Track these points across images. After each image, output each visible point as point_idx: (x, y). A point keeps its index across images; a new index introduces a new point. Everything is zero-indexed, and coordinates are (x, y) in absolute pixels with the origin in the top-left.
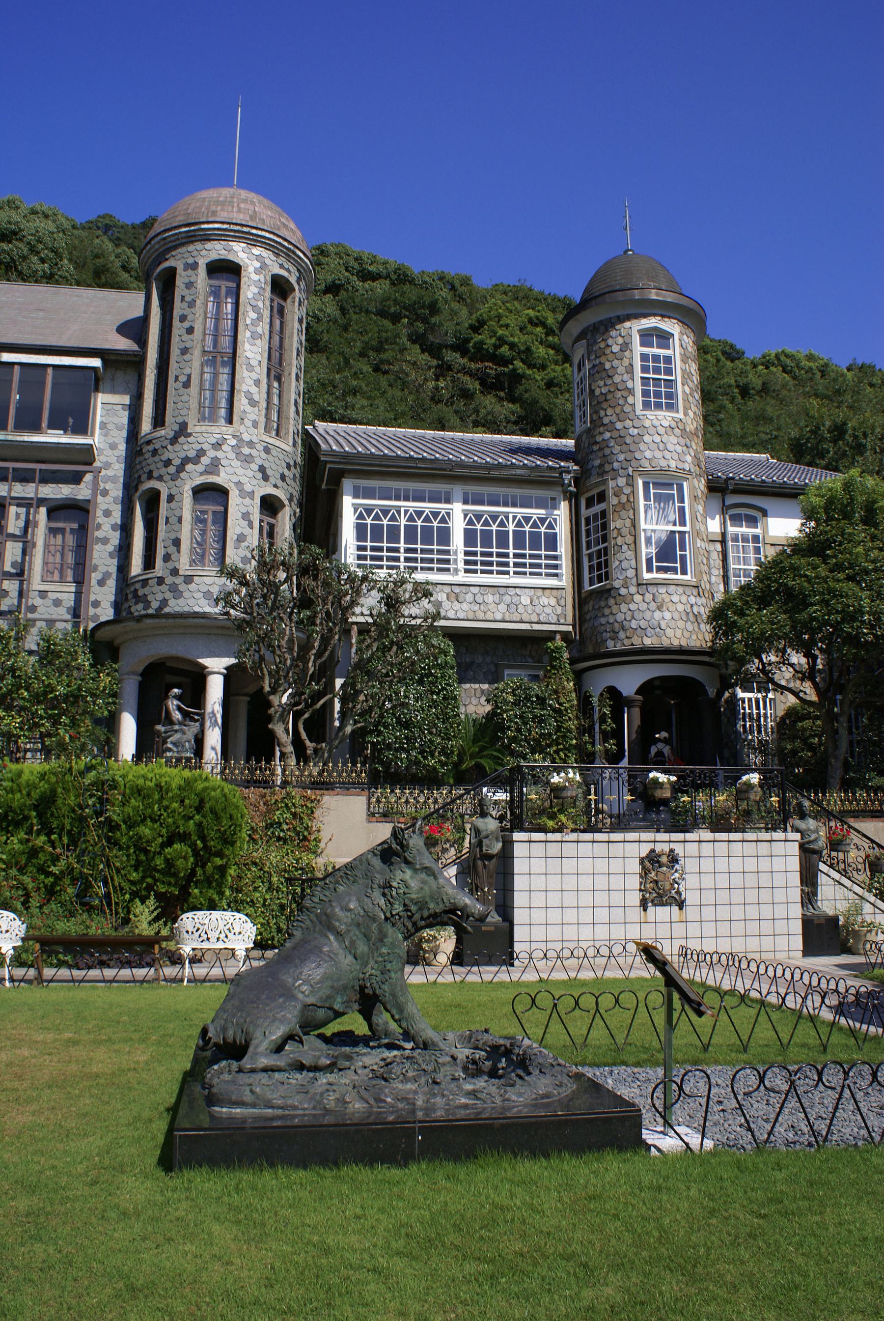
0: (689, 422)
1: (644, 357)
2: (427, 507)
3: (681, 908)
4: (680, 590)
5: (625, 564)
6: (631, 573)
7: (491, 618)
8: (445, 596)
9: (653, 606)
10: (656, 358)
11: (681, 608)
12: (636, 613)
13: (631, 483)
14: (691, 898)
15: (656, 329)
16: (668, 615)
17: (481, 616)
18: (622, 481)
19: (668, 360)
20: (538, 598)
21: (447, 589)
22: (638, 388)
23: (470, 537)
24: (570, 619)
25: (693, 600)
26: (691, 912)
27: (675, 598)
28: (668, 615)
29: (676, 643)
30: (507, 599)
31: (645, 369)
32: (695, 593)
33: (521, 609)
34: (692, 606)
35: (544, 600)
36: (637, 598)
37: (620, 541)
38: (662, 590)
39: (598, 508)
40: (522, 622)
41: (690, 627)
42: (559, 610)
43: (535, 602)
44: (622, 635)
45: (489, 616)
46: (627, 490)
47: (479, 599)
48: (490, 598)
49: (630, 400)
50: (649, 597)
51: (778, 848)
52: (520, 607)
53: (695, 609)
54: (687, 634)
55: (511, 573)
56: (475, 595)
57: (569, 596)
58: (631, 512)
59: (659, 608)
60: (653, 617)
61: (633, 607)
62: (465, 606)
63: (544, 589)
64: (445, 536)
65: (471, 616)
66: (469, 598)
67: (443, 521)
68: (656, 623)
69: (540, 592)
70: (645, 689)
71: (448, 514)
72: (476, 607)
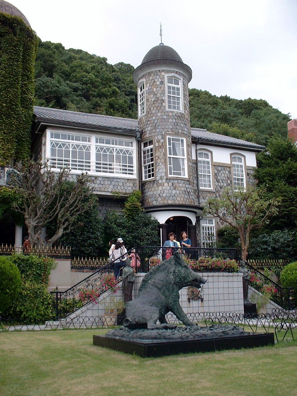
1: (169, 87)
2: (81, 143)
3: (202, 302)
4: (183, 182)
5: (160, 171)
6: (163, 174)
7: (107, 191)
9: (172, 188)
10: (174, 88)
11: (183, 189)
13: (164, 137)
14: (205, 298)
15: (174, 77)
16: (178, 192)
17: (103, 189)
18: (160, 137)
19: (178, 89)
20: (126, 183)
22: (166, 99)
23: (98, 157)
25: (187, 186)
26: (205, 303)
27: (181, 185)
28: (178, 192)
29: (181, 203)
30: (113, 183)
31: (169, 92)
32: (188, 183)
33: (119, 188)
34: (187, 188)
35: (128, 184)
36: (166, 184)
37: (159, 161)
38: (176, 182)
39: (149, 147)
44: (159, 199)
45: (106, 190)
46: (162, 141)
47: (102, 183)
48: (106, 183)
49: (164, 104)
50: (170, 184)
51: (235, 279)
52: (119, 187)
53: (188, 190)
54: (185, 200)
56: (100, 181)
58: (164, 149)
59: (175, 189)
60: (172, 192)
63: (128, 179)
64: (88, 156)
65: (99, 190)
66: (98, 182)
67: (87, 149)
69: (126, 181)
70: (168, 221)
71: (90, 147)
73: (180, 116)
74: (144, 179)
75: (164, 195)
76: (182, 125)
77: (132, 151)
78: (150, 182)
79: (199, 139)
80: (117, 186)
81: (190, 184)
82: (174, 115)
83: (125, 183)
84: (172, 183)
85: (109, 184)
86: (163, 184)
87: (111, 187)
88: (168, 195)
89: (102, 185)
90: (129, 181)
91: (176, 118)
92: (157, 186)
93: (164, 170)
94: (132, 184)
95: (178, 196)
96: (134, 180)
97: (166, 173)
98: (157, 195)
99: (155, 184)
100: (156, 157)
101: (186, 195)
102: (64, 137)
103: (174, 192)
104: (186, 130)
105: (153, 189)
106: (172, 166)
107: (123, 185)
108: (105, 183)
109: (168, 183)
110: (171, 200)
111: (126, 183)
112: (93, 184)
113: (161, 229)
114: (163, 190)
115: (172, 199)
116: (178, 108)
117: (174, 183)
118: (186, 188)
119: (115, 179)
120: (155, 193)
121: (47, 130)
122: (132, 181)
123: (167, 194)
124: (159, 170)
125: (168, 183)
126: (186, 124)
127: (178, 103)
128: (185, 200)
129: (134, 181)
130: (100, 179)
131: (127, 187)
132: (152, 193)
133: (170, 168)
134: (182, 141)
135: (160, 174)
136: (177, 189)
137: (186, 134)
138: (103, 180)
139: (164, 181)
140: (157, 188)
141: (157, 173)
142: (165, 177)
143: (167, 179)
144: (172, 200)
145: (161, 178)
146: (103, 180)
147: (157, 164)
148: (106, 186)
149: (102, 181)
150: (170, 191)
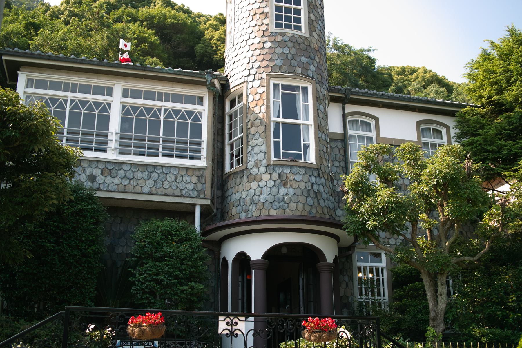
0: (314, 41)
4: (303, 171)
5: (256, 150)
6: (261, 156)
8: (99, 171)
11: (302, 185)
12: (264, 189)
16: (291, 191)
17: (130, 188)
20: (182, 176)
21: (101, 166)
24: (209, 193)
25: (313, 179)
29: (299, 213)
30: (155, 175)
32: (315, 174)
34: (312, 185)
35: (187, 178)
36: (266, 177)
37: (253, 131)
38: (287, 171)
40: (166, 195)
41: (310, 201)
42: (200, 186)
43: (179, 179)
48: (139, 175)
50: (275, 176)
52: (166, 183)
53: (315, 187)
55: (160, 154)
57: (208, 175)
59: (285, 185)
60: (278, 193)
61: (262, 184)
62: (117, 181)
64: (105, 121)
65: (121, 188)
66: (121, 173)
68: (282, 197)
70: (271, 254)
71: (109, 105)
72: (126, 182)
73: (300, 40)
74: (227, 169)
75: (262, 199)
76: (303, 59)
77: (201, 114)
78: (236, 173)
79: (347, 91)
80: (163, 182)
81: (321, 175)
82: (287, 39)
83: (180, 175)
84: (280, 174)
85: (146, 178)
86: (260, 176)
87: (150, 183)
88: (270, 198)
89: (128, 181)
90: (190, 172)
91: (290, 44)
92: (248, 181)
93: (264, 148)
94: (197, 178)
95: (291, 200)
96: (199, 169)
97: (267, 153)
98: (248, 199)
99: (245, 177)
100: (248, 122)
101: (310, 198)
102: (55, 86)
103: (282, 191)
104: (312, 68)
105: (241, 187)
106: (281, 140)
107: (176, 180)
108: (136, 177)
109: (271, 174)
110: (275, 208)
111: (182, 176)
112: (109, 177)
113: (253, 271)
114: (259, 189)
115: (278, 206)
116: (299, 28)
117: (282, 173)
118: (310, 184)
119: (158, 168)
120: (244, 196)
121: (18, 72)
122: (197, 173)
123: (269, 197)
124: (253, 148)
125: (271, 174)
126: (313, 58)
127: (298, 20)
128: (308, 208)
129: (201, 172)
130: (126, 168)
131: (184, 184)
132: (238, 196)
133: (277, 144)
134: (305, 89)
135: (255, 155)
136: (288, 185)
137: (313, 77)
138: (132, 171)
139: (262, 169)
140: (248, 184)
141: (249, 155)
142: (264, 162)
143: (268, 165)
144: (277, 209)
145: (256, 165)
146: (132, 171)
147: (250, 136)
148: (140, 182)
149: (130, 171)
150: (275, 189)
